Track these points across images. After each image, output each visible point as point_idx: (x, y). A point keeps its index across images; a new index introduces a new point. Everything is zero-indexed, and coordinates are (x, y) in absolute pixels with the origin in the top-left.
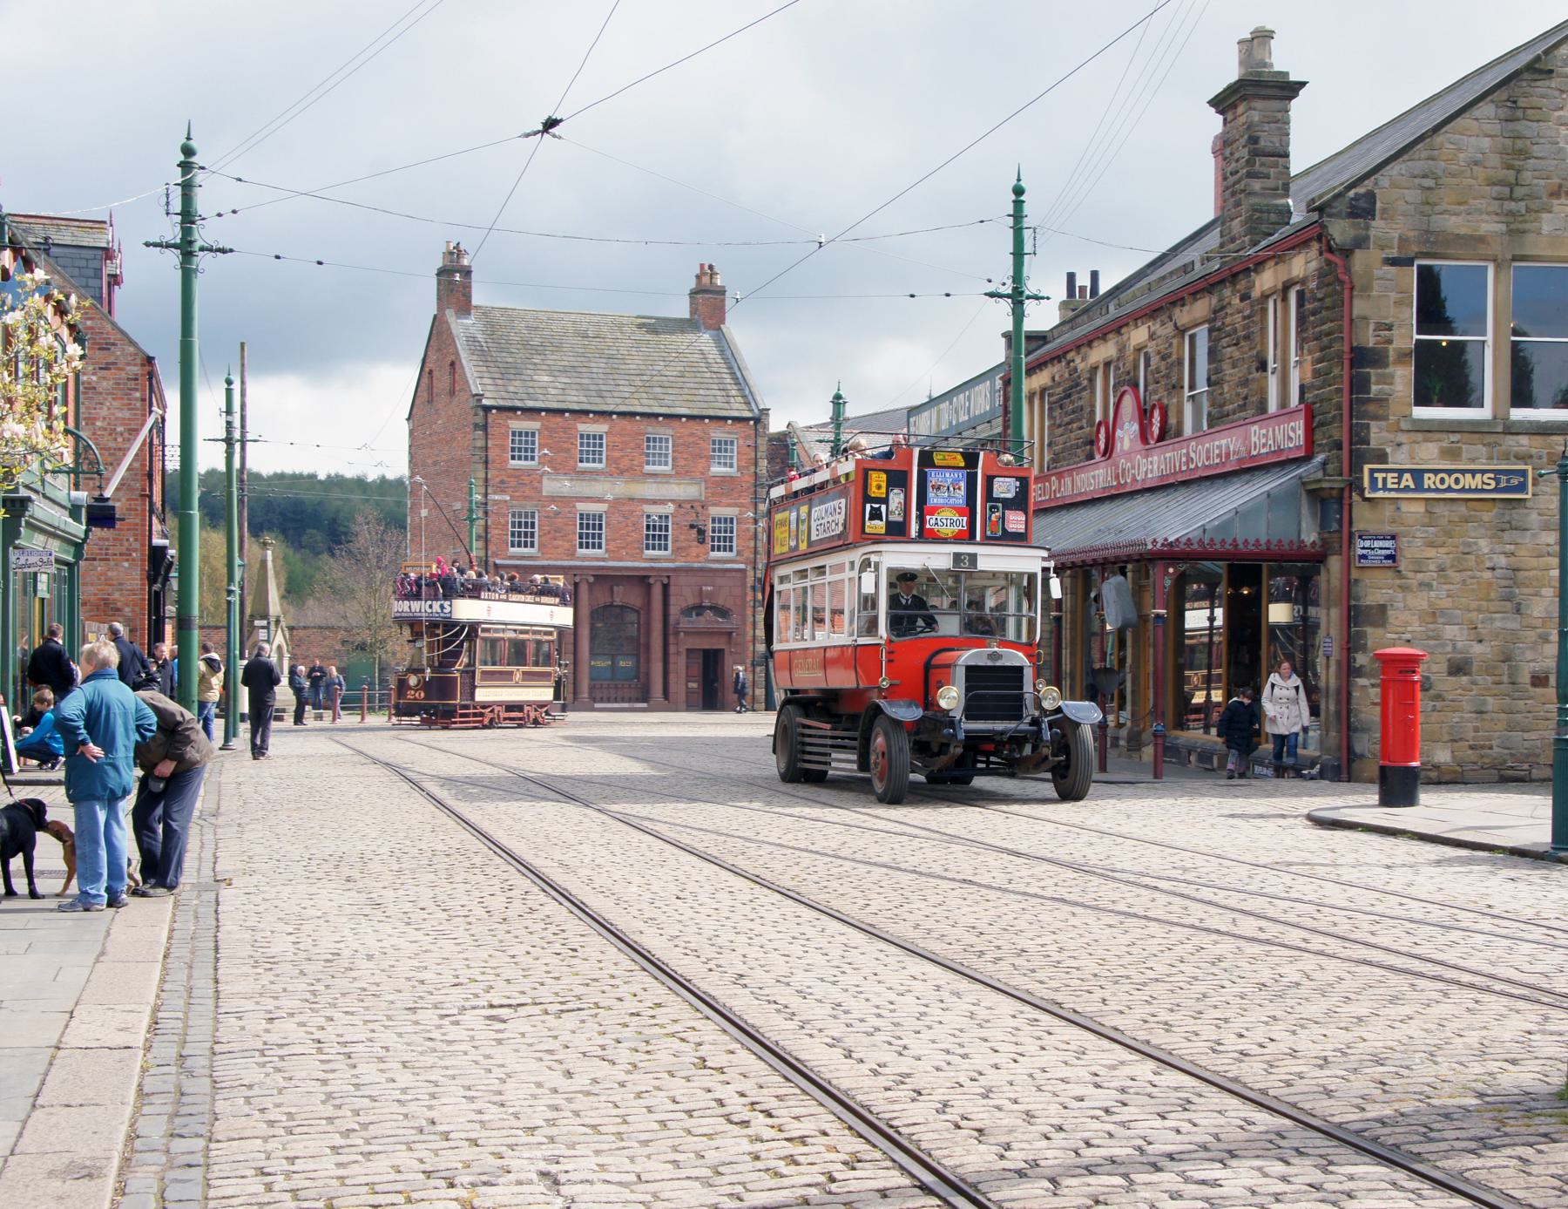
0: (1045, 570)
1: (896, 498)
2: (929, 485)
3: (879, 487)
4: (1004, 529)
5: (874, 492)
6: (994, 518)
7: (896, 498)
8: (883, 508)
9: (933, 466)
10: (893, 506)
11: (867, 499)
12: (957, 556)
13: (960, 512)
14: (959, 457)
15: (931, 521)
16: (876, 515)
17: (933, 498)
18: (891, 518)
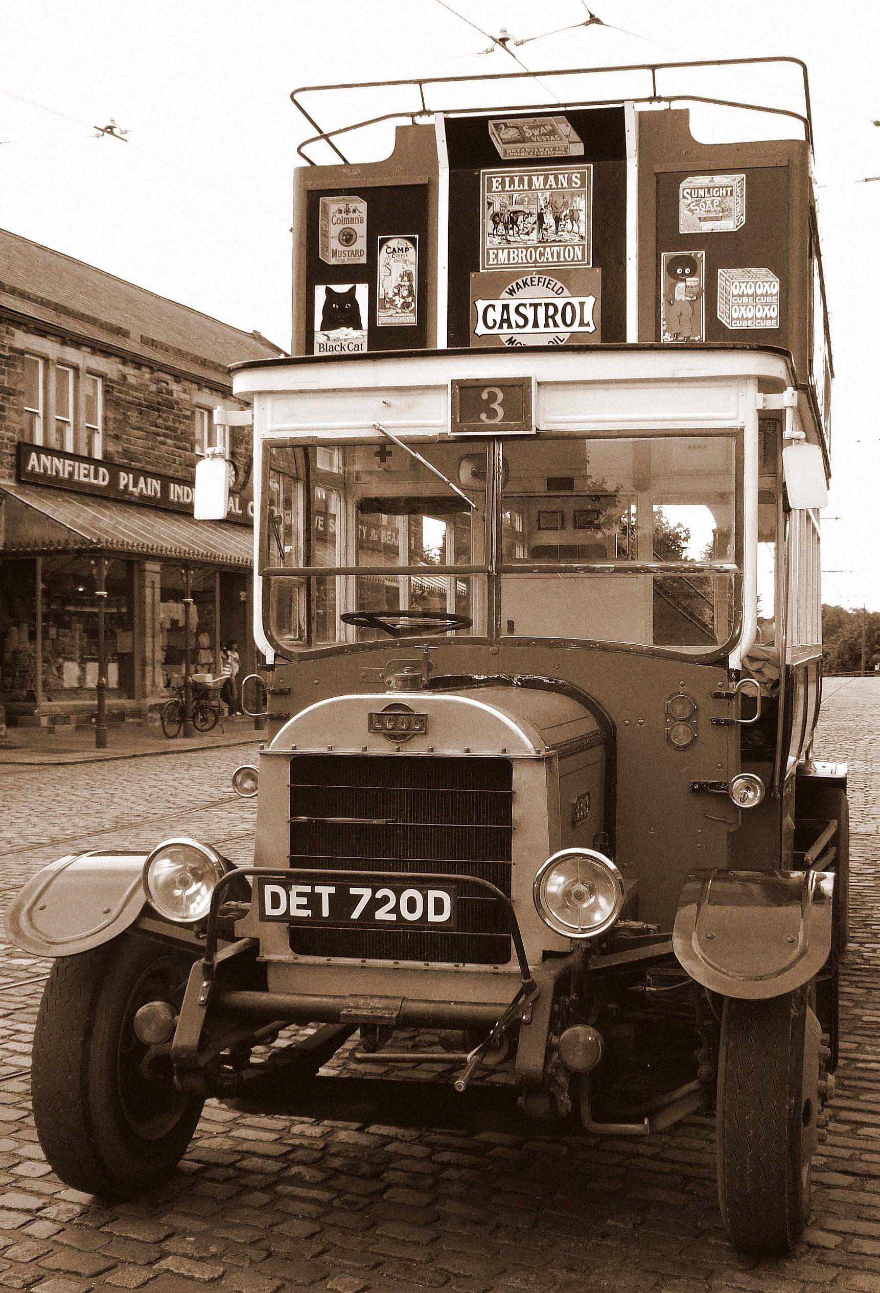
0: (771, 423)
1: (396, 264)
3: (348, 238)
4: (714, 326)
7: (396, 264)
8: (362, 292)
9: (495, 161)
12: (468, 395)
14: (565, 128)
15: (487, 313)
16: (342, 313)
17: (497, 253)
18: (384, 319)
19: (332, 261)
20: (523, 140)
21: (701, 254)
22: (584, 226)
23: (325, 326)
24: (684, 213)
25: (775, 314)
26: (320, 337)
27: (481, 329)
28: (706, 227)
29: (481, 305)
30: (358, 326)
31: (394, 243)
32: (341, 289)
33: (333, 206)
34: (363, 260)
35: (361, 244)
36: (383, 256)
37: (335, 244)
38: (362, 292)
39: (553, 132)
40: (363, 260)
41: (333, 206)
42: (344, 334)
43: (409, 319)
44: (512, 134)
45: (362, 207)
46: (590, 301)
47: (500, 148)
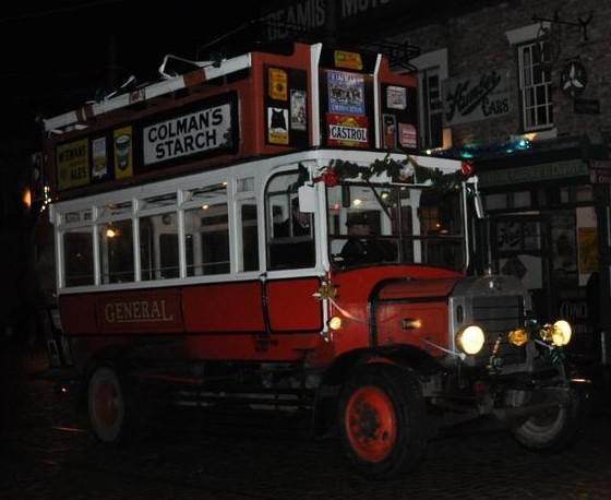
2: (330, 88)
3: (280, 88)
5: (276, 94)
6: (389, 132)
7: (297, 104)
8: (286, 113)
9: (333, 67)
10: (295, 112)
11: (269, 102)
13: (360, 123)
15: (334, 130)
17: (336, 107)
18: (294, 127)
19: (275, 97)
20: (344, 60)
21: (394, 117)
22: (361, 100)
23: (273, 126)
24: (389, 100)
25: (415, 142)
26: (271, 131)
27: (331, 137)
28: (396, 106)
29: (331, 127)
30: (285, 128)
31: (297, 94)
32: (279, 110)
33: (274, 73)
34: (286, 99)
35: (285, 92)
36: (293, 99)
37: (275, 90)
38: (286, 113)
39: (354, 60)
40: (286, 99)
41: (274, 73)
42: (279, 130)
43: (303, 128)
44: (342, 57)
45: (284, 76)
46: (365, 130)
47: (336, 62)
